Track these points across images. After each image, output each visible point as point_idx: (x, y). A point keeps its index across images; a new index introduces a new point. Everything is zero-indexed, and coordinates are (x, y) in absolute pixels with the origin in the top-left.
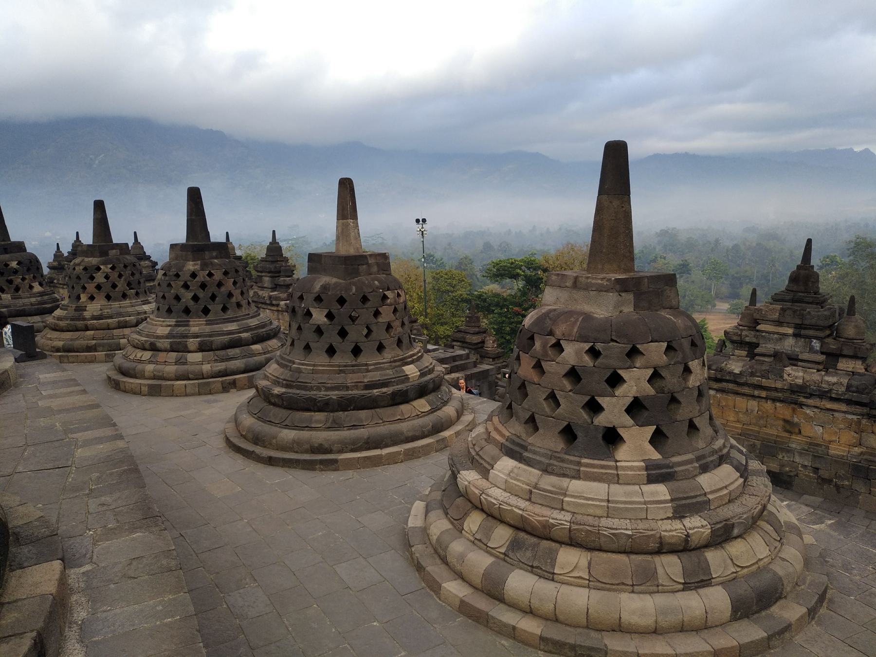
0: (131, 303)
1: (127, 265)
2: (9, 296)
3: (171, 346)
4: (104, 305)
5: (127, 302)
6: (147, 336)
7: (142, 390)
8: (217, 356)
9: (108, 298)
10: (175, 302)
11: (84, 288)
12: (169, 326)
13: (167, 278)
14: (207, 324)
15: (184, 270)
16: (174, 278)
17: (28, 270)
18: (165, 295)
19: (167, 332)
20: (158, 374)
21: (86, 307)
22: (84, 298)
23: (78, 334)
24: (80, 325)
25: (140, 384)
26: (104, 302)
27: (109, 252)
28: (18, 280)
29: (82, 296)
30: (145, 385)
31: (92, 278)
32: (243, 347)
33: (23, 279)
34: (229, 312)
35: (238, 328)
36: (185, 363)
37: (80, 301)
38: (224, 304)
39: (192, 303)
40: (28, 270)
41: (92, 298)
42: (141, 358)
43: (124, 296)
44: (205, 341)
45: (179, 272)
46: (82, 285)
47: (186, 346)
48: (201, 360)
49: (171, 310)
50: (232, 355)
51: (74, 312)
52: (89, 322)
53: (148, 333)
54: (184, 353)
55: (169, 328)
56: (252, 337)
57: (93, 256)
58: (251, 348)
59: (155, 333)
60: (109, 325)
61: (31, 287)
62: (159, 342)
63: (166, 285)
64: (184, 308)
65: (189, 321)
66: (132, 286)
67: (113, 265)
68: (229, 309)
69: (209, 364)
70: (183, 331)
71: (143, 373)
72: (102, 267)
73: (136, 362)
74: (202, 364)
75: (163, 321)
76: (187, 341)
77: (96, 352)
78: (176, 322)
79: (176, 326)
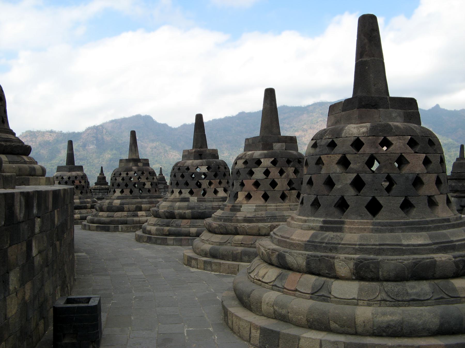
0: (290, 206)
1: (290, 159)
2: (196, 198)
3: (308, 264)
4: (259, 206)
5: (286, 204)
6: (279, 242)
7: (252, 335)
8: (386, 293)
9: (266, 197)
10: (324, 189)
11: (242, 185)
12: (312, 228)
13: (318, 150)
14: (373, 231)
15: (343, 135)
16: (327, 150)
17: (216, 175)
18: (313, 179)
19: (306, 239)
20: (280, 310)
21: (241, 207)
22: (241, 196)
23: (227, 237)
24: (230, 228)
25: (251, 323)
26: (261, 202)
27: (274, 144)
28: (205, 183)
29: (239, 194)
30: (257, 327)
31: (251, 173)
32: (436, 281)
33: (210, 184)
34: (414, 212)
35: (430, 242)
36: (325, 299)
37: (237, 200)
38: (406, 197)
39: (352, 191)
40: (216, 175)
41: (249, 197)
42: (263, 277)
43: (283, 197)
44: (365, 259)
45: (335, 140)
46: (241, 181)
47: (332, 267)
48: (356, 297)
49: (319, 203)
50: (416, 294)
51: (229, 212)
52: (239, 225)
53: (280, 238)
54: (328, 279)
55: (312, 232)
56: (455, 263)
57: (256, 149)
58: (453, 284)
59: (288, 238)
60: (259, 230)
61: (216, 192)
62: (290, 254)
63: (315, 161)
64: (338, 199)
65: (343, 223)
66: (294, 186)
67: (275, 158)
68: (414, 207)
69: (369, 305)
70: (332, 238)
71: (259, 304)
72: (262, 160)
73: (256, 283)
74: (357, 305)
75: (305, 221)
76: (334, 258)
77: (241, 262)
78: (324, 222)
79: (322, 228)
